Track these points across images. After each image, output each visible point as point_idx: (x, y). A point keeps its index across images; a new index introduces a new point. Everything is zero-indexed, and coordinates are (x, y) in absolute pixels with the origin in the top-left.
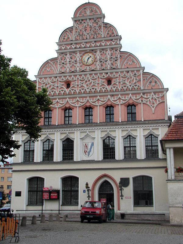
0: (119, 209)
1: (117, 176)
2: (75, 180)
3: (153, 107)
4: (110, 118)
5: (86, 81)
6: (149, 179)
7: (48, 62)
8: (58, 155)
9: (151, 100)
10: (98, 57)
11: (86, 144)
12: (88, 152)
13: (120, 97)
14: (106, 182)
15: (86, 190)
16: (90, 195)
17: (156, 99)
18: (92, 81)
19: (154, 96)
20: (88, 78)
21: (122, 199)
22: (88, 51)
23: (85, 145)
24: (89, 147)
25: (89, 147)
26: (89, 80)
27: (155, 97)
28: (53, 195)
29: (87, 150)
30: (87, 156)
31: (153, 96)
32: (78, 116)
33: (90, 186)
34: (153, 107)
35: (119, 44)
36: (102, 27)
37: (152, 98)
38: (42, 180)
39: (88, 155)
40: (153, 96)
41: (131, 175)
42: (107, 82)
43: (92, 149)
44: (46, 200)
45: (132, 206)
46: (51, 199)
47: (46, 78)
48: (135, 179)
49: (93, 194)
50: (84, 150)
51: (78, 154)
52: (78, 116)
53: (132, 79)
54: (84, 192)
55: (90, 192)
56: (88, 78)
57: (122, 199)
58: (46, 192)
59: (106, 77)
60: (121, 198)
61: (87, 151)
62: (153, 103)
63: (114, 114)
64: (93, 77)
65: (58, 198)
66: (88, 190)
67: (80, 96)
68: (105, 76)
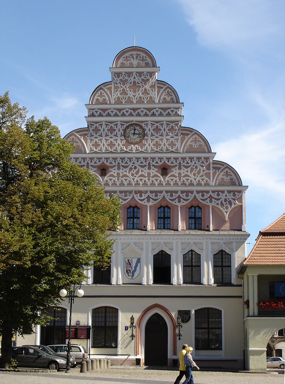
1: (174, 308)
3: (226, 212)
4: (164, 223)
5: (131, 169)
6: (218, 313)
7: (73, 134)
10: (149, 134)
11: (128, 260)
12: (131, 272)
14: (157, 315)
19: (228, 196)
20: (134, 163)
21: (180, 339)
22: (134, 122)
23: (127, 261)
24: (134, 265)
25: (134, 265)
26: (135, 168)
29: (130, 269)
31: (226, 196)
34: (226, 212)
36: (156, 87)
37: (226, 200)
39: (132, 276)
40: (226, 196)
41: (193, 306)
42: (160, 171)
43: (138, 268)
50: (125, 269)
53: (198, 169)
54: (125, 329)
56: (134, 163)
57: (180, 339)
59: (160, 164)
60: (178, 338)
61: (130, 271)
63: (170, 218)
64: (142, 163)
67: (123, 189)
68: (159, 162)
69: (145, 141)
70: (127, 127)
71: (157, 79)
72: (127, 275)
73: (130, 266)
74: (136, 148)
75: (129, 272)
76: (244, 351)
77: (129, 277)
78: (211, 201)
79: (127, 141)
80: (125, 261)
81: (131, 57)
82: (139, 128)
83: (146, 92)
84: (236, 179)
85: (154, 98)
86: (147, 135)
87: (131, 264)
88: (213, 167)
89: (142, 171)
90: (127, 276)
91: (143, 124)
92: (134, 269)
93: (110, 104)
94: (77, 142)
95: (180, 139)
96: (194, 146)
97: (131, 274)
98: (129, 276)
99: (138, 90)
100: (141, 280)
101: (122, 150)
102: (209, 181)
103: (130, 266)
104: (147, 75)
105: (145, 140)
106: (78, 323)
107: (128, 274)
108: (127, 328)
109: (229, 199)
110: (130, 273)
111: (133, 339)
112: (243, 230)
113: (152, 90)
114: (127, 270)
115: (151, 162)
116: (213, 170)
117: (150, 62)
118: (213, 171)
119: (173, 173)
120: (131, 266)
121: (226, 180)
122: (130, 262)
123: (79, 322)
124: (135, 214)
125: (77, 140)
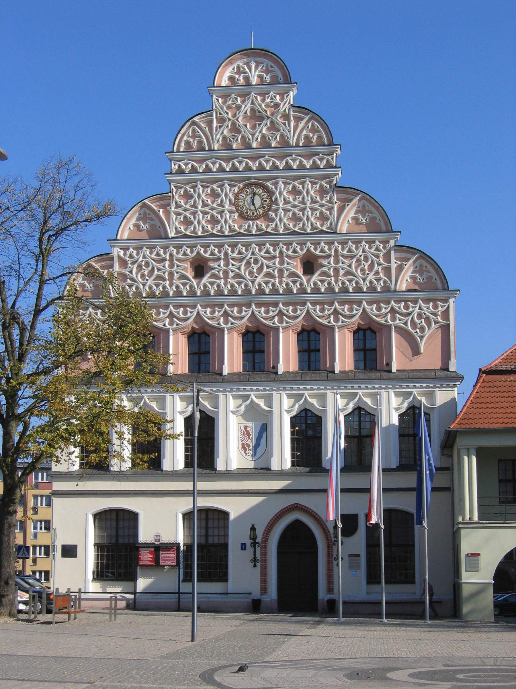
3: (421, 337)
4: (309, 361)
8: (175, 454)
12: (251, 447)
13: (338, 307)
14: (297, 523)
15: (248, 542)
16: (258, 556)
17: (427, 319)
18: (265, 261)
22: (253, 181)
23: (243, 429)
27: (426, 312)
29: (248, 442)
30: (249, 458)
33: (260, 533)
35: (336, 167)
37: (420, 316)
38: (132, 517)
43: (263, 441)
45: (365, 582)
49: (264, 553)
50: (240, 443)
54: (242, 549)
55: (258, 550)
58: (147, 546)
61: (248, 446)
62: (422, 329)
66: (254, 544)
69: (274, 214)
70: (241, 191)
71: (292, 103)
72: (243, 452)
73: (249, 437)
74: (257, 226)
75: (247, 448)
76: (454, 585)
77: (247, 457)
78: (394, 319)
79: (241, 216)
80: (239, 429)
82: (261, 191)
83: (273, 127)
84: (437, 279)
85: (288, 138)
86: (276, 202)
88: (396, 258)
90: (244, 455)
93: (210, 150)
94: (152, 219)
95: (335, 209)
96: (362, 220)
97: (251, 452)
98: (246, 454)
99: (259, 125)
100: (269, 461)
101: (231, 230)
102: (389, 282)
103: (249, 437)
104: (275, 97)
105: (273, 211)
106: (158, 538)
107: (245, 452)
108: (245, 546)
109: (425, 314)
110: (249, 450)
111: (255, 566)
112: (450, 370)
113: (285, 124)
114: (243, 444)
115: (284, 250)
116: (395, 263)
117: (280, 76)
118: (396, 265)
119: (325, 269)
122: (249, 429)
123: (159, 536)
124: (257, 344)
125: (152, 215)
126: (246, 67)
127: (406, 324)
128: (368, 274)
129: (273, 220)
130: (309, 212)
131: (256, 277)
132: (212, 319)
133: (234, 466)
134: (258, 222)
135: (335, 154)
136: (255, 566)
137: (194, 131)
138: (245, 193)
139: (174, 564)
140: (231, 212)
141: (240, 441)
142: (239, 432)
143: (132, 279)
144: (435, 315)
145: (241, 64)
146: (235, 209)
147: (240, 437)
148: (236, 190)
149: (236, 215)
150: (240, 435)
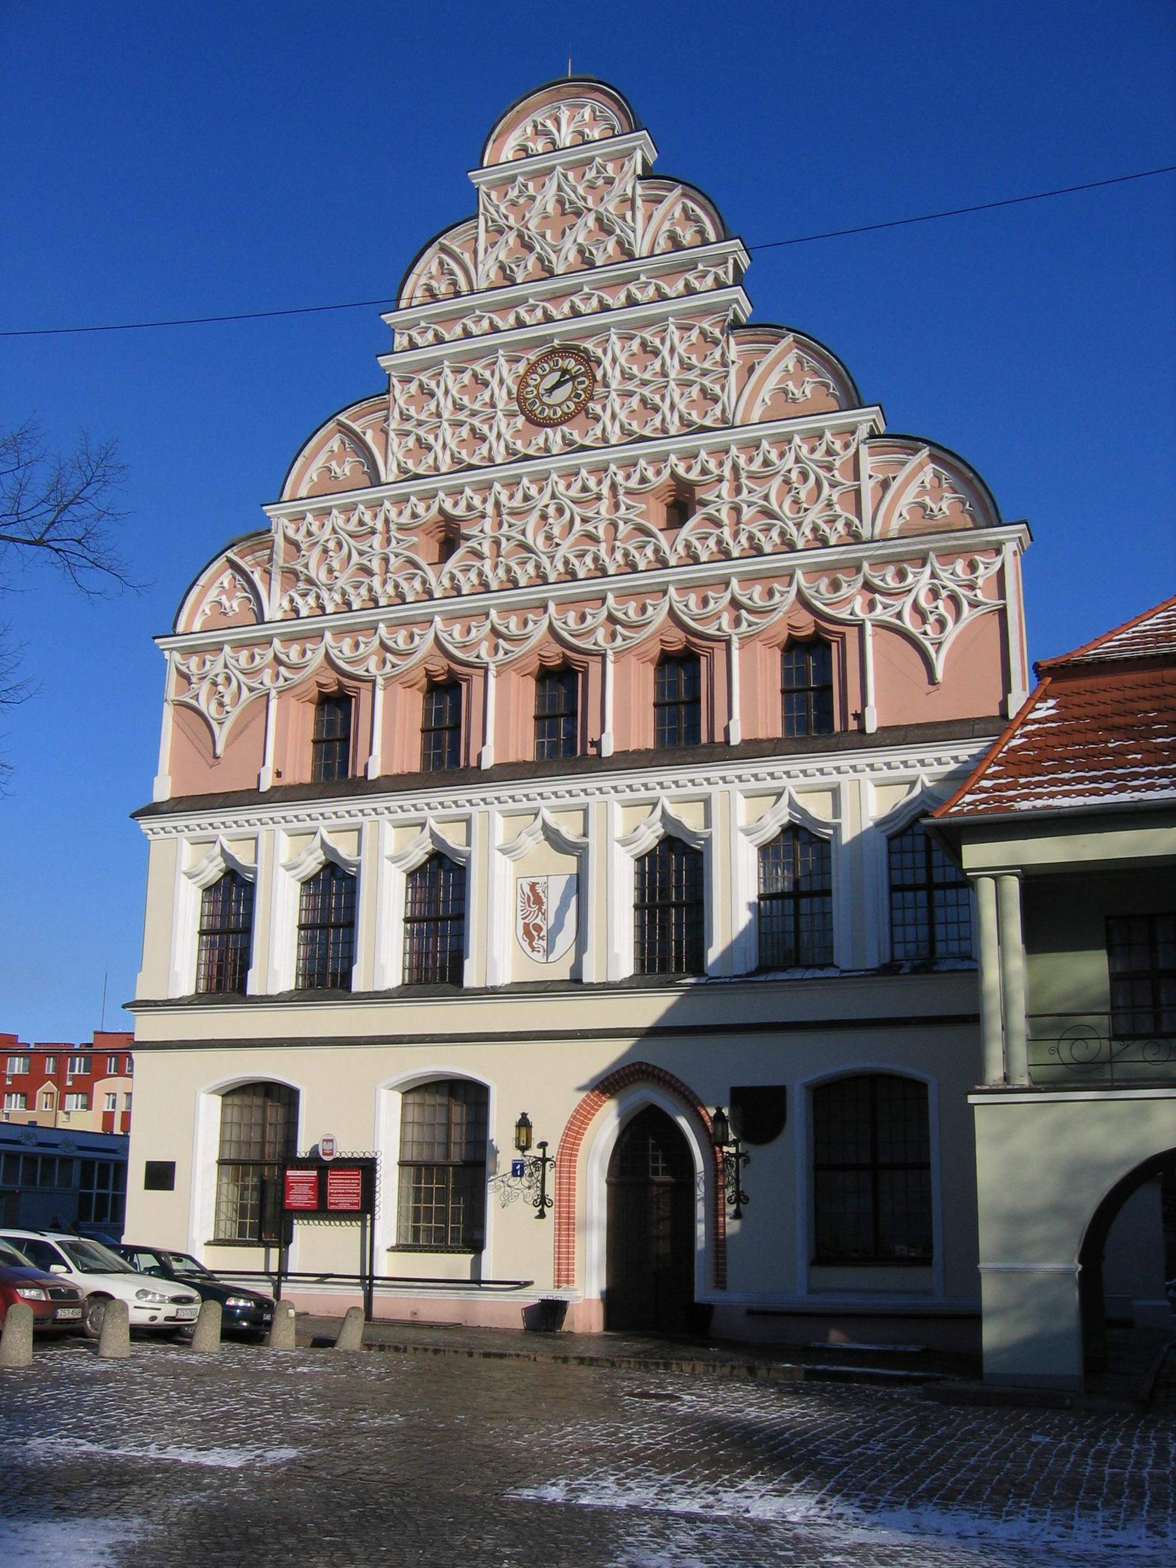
0: (720, 1282)
2: (468, 1096)
9: (923, 602)
11: (533, 886)
16: (550, 1191)
17: (954, 598)
23: (527, 889)
28: (342, 1188)
29: (538, 921)
32: (503, 721)
37: (934, 593)
39: (549, 951)
41: (796, 1067)
44: (307, 1214)
46: (321, 1210)
47: (327, 512)
48: (825, 1094)
50: (521, 923)
51: (496, 947)
52: (503, 721)
55: (551, 1175)
59: (656, 481)
61: (538, 928)
62: (942, 623)
65: (366, 1208)
70: (532, 368)
72: (525, 945)
73: (540, 909)
74: (563, 437)
75: (535, 934)
77: (535, 955)
79: (532, 420)
80: (519, 891)
81: (549, 123)
82: (573, 362)
85: (629, 243)
87: (545, 900)
89: (585, 520)
90: (528, 950)
91: (589, 345)
92: (556, 918)
93: (472, 292)
97: (544, 943)
98: (533, 949)
102: (856, 521)
103: (540, 909)
107: (530, 944)
109: (944, 588)
110: (540, 938)
111: (542, 1215)
114: (526, 926)
116: (871, 477)
118: (872, 483)
119: (710, 510)
120: (544, 907)
121: (932, 510)
122: (539, 891)
123: (331, 1141)
126: (549, 123)
127: (899, 615)
128: (806, 510)
129: (597, 419)
130: (674, 391)
131: (558, 545)
132: (464, 647)
133: (504, 976)
134: (564, 428)
135: (731, 261)
136: (542, 1215)
137: (441, 263)
138: (540, 371)
139: (356, 1207)
140: (511, 415)
141: (519, 917)
142: (519, 898)
143: (310, 581)
144: (972, 587)
145: (539, 120)
146: (517, 408)
147: (519, 908)
148: (521, 368)
149: (520, 421)
150: (520, 904)
